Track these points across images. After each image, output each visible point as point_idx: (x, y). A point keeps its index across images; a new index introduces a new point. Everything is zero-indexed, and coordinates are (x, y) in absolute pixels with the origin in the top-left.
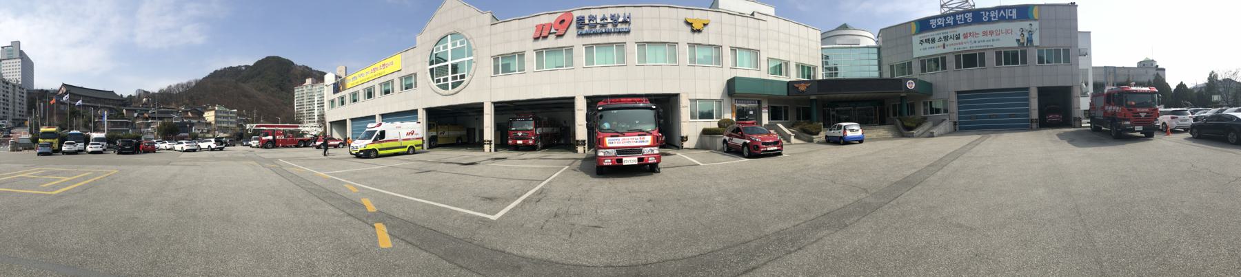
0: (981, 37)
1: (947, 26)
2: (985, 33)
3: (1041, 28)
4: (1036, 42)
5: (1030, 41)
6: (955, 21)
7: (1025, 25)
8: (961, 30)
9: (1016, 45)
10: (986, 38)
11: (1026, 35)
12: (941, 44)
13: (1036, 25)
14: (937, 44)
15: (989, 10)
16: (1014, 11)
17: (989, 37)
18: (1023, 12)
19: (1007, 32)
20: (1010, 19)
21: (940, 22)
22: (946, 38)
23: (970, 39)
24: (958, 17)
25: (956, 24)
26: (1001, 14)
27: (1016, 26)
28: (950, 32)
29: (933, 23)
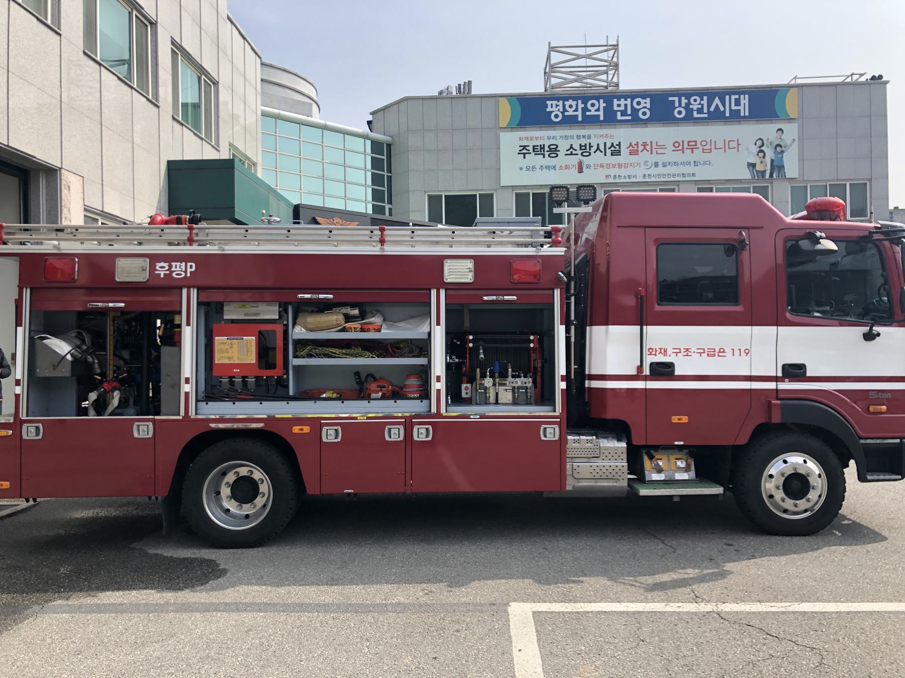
1: (590, 121)
2: (678, 146)
3: (801, 139)
4: (791, 169)
5: (777, 167)
7: (767, 130)
8: (624, 135)
9: (746, 174)
10: (678, 157)
11: (770, 154)
12: (574, 160)
13: (791, 131)
14: (562, 159)
15: (688, 94)
16: (745, 100)
17: (688, 156)
18: (764, 102)
20: (735, 117)
21: (574, 109)
22: (585, 150)
23: (644, 156)
24: (618, 105)
25: (610, 118)
26: (715, 106)
27: (749, 133)
28: (597, 135)
29: (554, 108)
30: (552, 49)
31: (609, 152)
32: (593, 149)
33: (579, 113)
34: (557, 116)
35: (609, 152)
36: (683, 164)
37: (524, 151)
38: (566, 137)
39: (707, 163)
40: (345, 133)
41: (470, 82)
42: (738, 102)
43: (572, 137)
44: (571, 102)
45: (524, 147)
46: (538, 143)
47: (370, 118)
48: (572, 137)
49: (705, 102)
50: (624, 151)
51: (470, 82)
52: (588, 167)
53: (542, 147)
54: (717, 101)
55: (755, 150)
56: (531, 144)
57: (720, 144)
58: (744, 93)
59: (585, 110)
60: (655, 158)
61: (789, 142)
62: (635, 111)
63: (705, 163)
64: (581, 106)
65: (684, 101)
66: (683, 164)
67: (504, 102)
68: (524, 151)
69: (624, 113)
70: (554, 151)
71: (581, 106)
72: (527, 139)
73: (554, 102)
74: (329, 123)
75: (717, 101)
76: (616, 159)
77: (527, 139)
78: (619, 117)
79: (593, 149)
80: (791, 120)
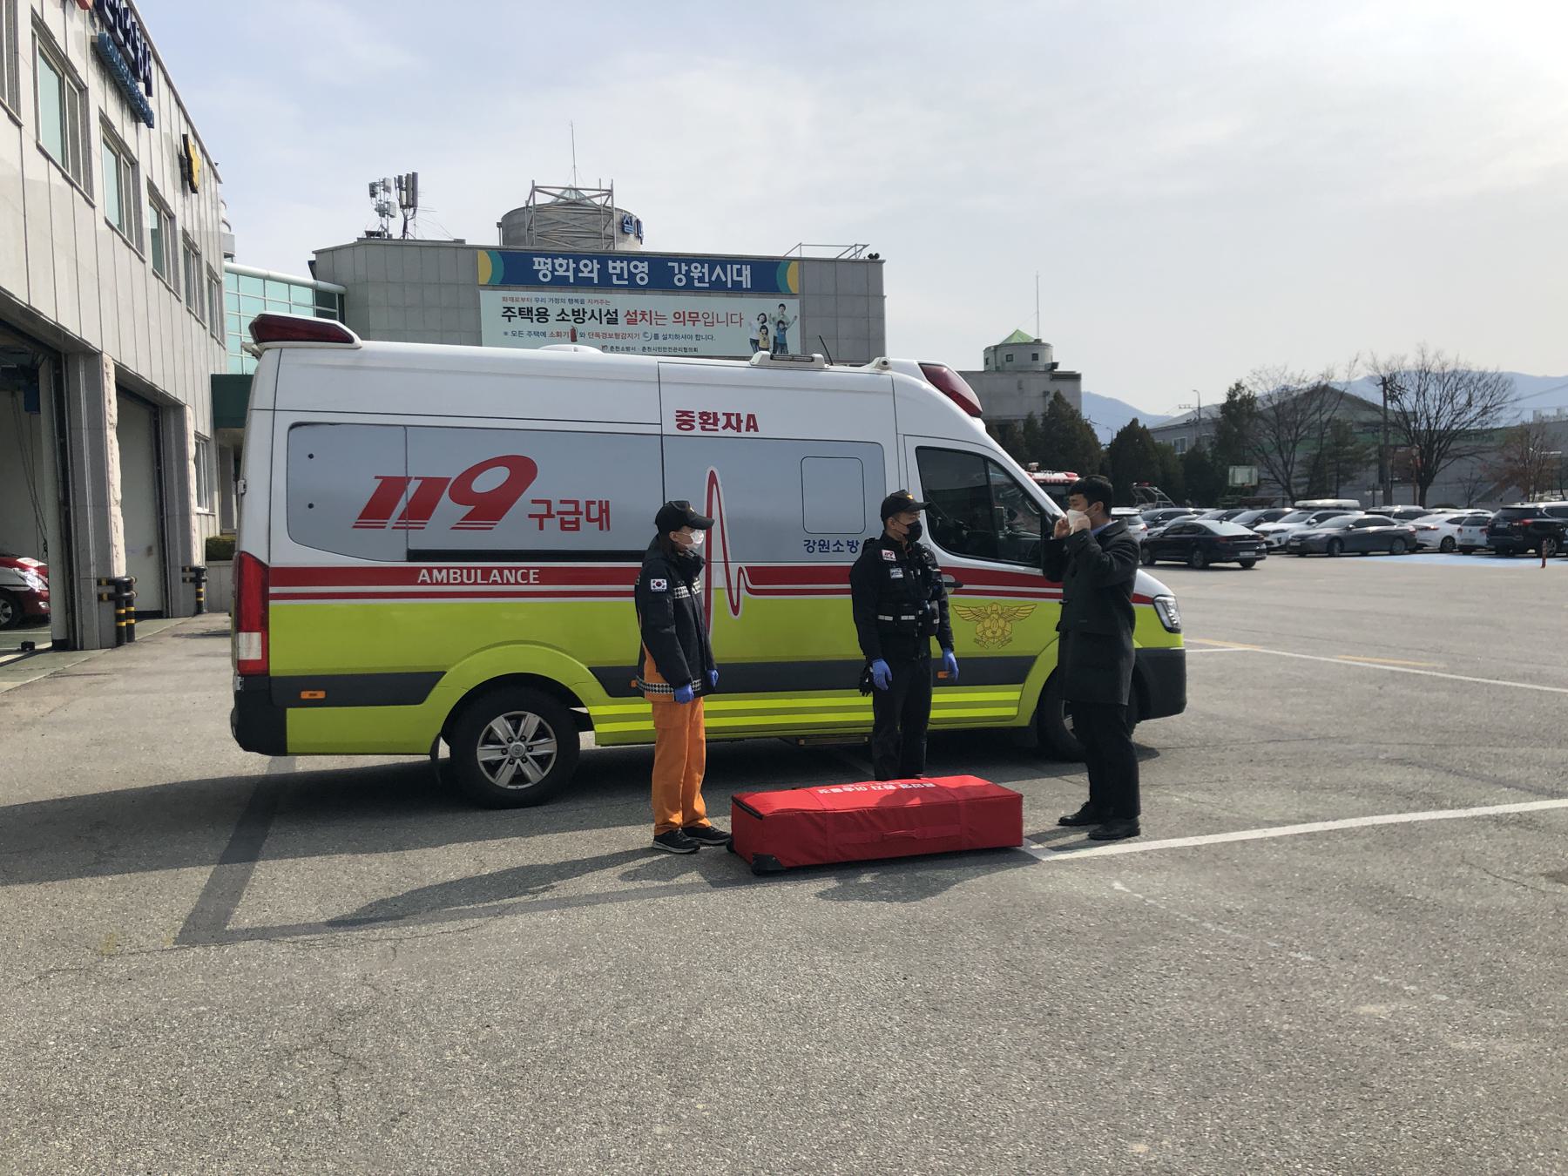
0: (672, 328)
1: (583, 284)
2: (679, 317)
6: (603, 272)
7: (770, 305)
8: (621, 302)
10: (679, 329)
12: (566, 327)
13: (793, 306)
14: (552, 325)
15: (689, 259)
16: (747, 271)
17: (689, 329)
19: (729, 318)
20: (737, 289)
21: (564, 268)
23: (642, 326)
24: (614, 267)
25: (605, 283)
28: (591, 301)
29: (542, 266)
30: (535, 189)
31: (604, 320)
32: (588, 316)
33: (571, 274)
34: (545, 276)
35: (604, 320)
36: (685, 337)
37: (508, 313)
38: (557, 301)
39: (709, 337)
40: (290, 283)
41: (415, 175)
42: (739, 273)
43: (563, 301)
44: (560, 260)
45: (509, 309)
46: (525, 305)
47: (313, 258)
48: (563, 301)
49: (706, 270)
50: (622, 319)
51: (415, 175)
52: (582, 335)
53: (530, 311)
54: (718, 270)
55: (758, 325)
56: (517, 305)
57: (722, 318)
58: (746, 263)
59: (577, 270)
60: (655, 329)
61: (791, 319)
62: (632, 276)
63: (707, 337)
64: (572, 266)
65: (684, 268)
66: (685, 337)
67: (482, 255)
68: (508, 313)
69: (620, 277)
70: (543, 315)
71: (572, 266)
72: (512, 299)
73: (542, 260)
74: (273, 273)
75: (718, 270)
76: (612, 329)
77: (512, 299)
78: (615, 282)
79: (588, 316)
80: (792, 295)
